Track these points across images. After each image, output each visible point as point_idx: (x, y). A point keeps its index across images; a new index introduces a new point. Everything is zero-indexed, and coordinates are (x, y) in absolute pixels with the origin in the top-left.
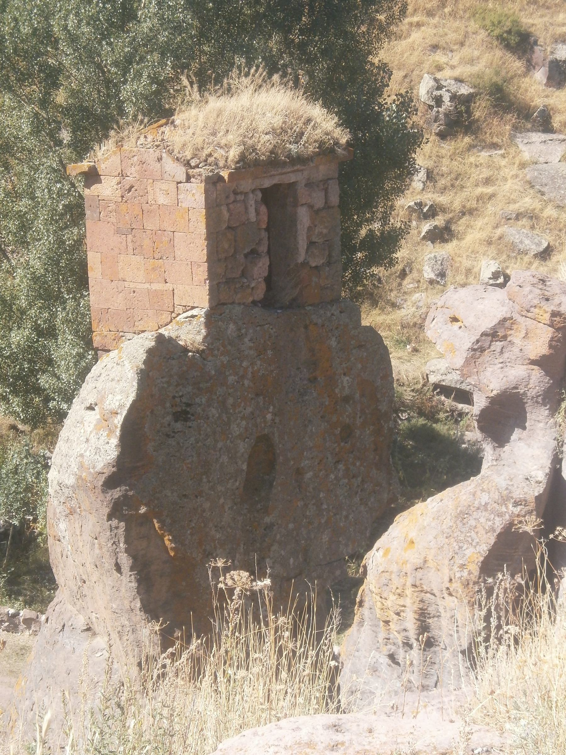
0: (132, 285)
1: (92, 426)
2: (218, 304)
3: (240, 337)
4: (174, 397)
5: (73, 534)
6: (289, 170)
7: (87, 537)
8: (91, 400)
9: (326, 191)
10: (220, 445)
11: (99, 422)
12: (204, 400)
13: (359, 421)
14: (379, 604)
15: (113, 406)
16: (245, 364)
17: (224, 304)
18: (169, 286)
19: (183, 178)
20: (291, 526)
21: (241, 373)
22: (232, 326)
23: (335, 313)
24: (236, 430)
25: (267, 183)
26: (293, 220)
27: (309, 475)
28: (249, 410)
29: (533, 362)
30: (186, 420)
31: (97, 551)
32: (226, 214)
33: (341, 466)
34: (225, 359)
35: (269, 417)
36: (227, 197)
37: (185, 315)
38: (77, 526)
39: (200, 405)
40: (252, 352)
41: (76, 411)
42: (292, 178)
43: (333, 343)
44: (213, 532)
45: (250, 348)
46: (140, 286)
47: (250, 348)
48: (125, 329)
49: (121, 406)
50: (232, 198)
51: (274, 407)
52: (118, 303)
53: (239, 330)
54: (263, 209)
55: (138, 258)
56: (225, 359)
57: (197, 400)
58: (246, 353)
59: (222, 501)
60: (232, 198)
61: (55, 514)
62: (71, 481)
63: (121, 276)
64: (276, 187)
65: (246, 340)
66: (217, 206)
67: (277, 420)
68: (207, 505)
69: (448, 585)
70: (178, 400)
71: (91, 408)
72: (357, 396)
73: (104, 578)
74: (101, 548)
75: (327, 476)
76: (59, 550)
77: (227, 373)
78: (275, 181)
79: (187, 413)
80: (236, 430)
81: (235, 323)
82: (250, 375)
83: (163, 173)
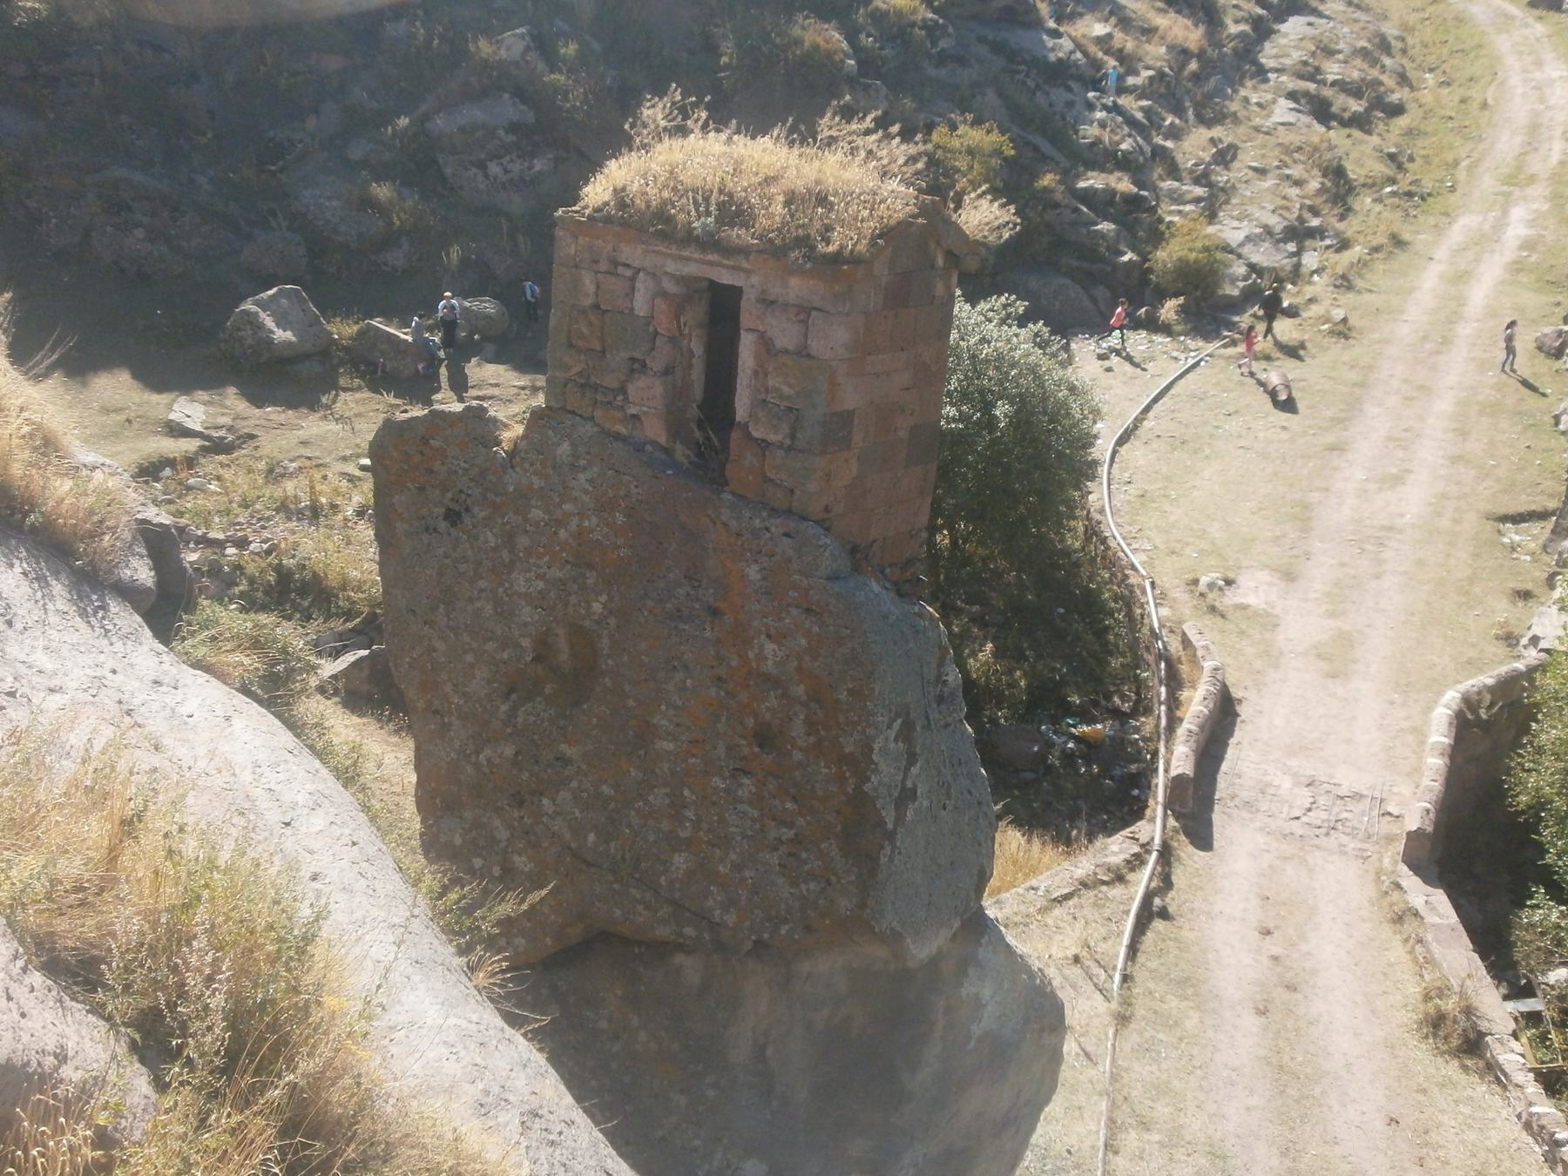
2: (563, 409)
3: (573, 467)
4: (461, 491)
6: (696, 256)
10: (482, 584)
16: (567, 507)
17: (573, 412)
21: (558, 514)
22: (565, 447)
23: (773, 529)
25: (671, 267)
28: (560, 575)
30: (454, 524)
34: (537, 483)
35: (597, 607)
36: (596, 262)
39: (473, 516)
40: (586, 499)
42: (726, 278)
43: (753, 572)
44: (448, 688)
45: (586, 492)
47: (586, 492)
50: (603, 266)
51: (611, 598)
53: (576, 457)
56: (537, 483)
59: (469, 658)
60: (603, 266)
65: (582, 477)
66: (576, 267)
70: (463, 496)
77: (533, 502)
79: (459, 514)
80: (520, 581)
81: (572, 444)
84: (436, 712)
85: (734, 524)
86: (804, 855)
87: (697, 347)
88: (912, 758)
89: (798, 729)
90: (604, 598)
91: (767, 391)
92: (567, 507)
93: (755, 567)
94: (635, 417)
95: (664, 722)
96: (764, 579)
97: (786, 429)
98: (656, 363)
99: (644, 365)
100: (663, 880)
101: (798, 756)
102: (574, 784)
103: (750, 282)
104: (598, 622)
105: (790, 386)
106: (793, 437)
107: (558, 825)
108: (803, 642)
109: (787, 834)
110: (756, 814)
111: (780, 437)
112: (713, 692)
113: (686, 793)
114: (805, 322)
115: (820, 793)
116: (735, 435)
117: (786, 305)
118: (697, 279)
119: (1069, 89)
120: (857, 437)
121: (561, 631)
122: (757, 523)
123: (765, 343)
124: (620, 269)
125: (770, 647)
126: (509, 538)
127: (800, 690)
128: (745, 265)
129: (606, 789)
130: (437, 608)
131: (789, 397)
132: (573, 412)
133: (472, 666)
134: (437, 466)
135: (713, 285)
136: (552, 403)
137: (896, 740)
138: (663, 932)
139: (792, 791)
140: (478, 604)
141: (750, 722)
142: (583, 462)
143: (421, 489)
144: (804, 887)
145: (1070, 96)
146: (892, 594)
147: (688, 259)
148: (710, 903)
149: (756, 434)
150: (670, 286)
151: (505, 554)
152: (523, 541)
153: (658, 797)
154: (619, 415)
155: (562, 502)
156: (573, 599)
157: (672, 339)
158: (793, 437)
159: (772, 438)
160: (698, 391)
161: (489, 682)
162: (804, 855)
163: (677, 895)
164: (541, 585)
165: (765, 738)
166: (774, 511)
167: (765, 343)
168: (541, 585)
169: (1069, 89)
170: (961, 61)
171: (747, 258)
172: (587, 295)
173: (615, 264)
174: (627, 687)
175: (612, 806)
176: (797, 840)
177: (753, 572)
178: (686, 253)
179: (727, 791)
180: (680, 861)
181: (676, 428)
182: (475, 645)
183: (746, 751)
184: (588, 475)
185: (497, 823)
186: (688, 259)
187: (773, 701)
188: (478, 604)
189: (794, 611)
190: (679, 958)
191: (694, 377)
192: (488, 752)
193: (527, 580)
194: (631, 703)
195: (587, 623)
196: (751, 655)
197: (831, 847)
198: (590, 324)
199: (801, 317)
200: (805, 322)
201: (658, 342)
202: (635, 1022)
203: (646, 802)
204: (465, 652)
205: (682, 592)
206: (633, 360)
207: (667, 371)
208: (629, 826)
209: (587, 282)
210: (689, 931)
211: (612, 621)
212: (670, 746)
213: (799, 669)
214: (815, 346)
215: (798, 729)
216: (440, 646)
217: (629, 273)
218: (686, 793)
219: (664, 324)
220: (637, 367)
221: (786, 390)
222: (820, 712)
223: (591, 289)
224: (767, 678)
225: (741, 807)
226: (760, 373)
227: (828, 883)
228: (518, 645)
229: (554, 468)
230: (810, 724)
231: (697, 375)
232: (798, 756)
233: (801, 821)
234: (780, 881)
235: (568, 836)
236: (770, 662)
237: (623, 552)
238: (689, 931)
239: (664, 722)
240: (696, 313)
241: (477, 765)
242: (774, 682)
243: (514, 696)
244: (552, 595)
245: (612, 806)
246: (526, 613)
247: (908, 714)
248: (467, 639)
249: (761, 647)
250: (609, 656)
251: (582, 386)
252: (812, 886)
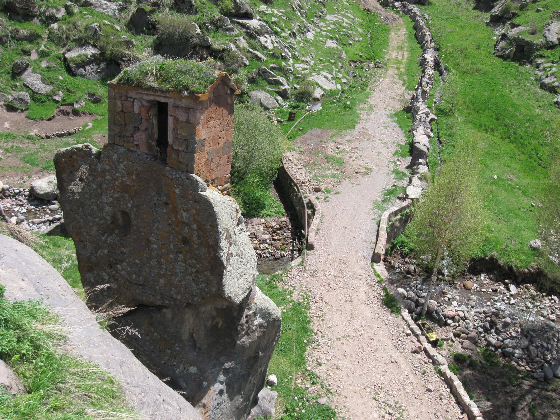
2: (114, 143)
6: (153, 94)
10: (93, 200)
16: (118, 174)
21: (115, 177)
25: (145, 97)
28: (117, 196)
32: (119, 104)
35: (129, 205)
40: (123, 172)
42: (162, 100)
43: (177, 191)
44: (85, 234)
45: (123, 169)
47: (123, 169)
51: (134, 202)
56: (108, 168)
58: (120, 170)
59: (91, 224)
60: (123, 98)
65: (121, 165)
67: (135, 209)
80: (104, 199)
81: (118, 155)
82: (120, 181)
84: (82, 241)
85: (170, 176)
86: (200, 276)
87: (155, 122)
88: (231, 245)
89: (195, 238)
90: (131, 202)
91: (178, 134)
92: (118, 174)
93: (178, 189)
94: (137, 145)
95: (153, 239)
96: (181, 193)
97: (184, 146)
98: (142, 128)
99: (138, 128)
100: (157, 287)
101: (195, 246)
102: (127, 260)
103: (171, 102)
104: (130, 210)
105: (185, 133)
106: (187, 148)
107: (123, 273)
108: (195, 212)
109: (194, 270)
110: (184, 265)
111: (183, 149)
112: (168, 229)
113: (162, 260)
114: (188, 113)
115: (203, 257)
116: (169, 149)
117: (182, 107)
118: (153, 101)
119: (265, 37)
120: (207, 147)
121: (119, 214)
122: (178, 176)
123: (176, 119)
124: (129, 99)
125: (184, 214)
126: (100, 185)
127: (195, 226)
128: (168, 95)
129: (137, 261)
130: (79, 209)
131: (184, 136)
132: (117, 145)
133: (92, 226)
134: (75, 164)
135: (159, 103)
136: (110, 142)
137: (225, 240)
138: (159, 303)
139: (195, 257)
140: (92, 207)
141: (180, 237)
142: (121, 160)
143: (71, 172)
144: (200, 286)
145: (266, 39)
146: (221, 195)
147: (150, 95)
148: (172, 293)
149: (175, 148)
150: (145, 104)
151: (99, 191)
152: (105, 186)
153: (154, 262)
154: (132, 145)
155: (116, 173)
156: (122, 203)
157: (147, 120)
158: (187, 148)
159: (180, 149)
160: (156, 136)
161: (98, 231)
162: (200, 276)
163: (162, 291)
164: (111, 199)
165: (186, 241)
166: (182, 172)
167: (176, 119)
168: (111, 199)
169: (265, 37)
170: (231, 30)
171: (169, 93)
172: (119, 108)
173: (127, 97)
174: (141, 229)
175: (140, 266)
176: (197, 272)
177: (177, 191)
178: (149, 93)
179: (175, 259)
180: (162, 281)
181: (150, 147)
182: (92, 220)
183: (179, 246)
184: (123, 164)
185: (104, 274)
186: (150, 95)
187: (186, 230)
188: (92, 207)
189: (191, 202)
190: (164, 310)
191: (155, 131)
192: (99, 252)
193: (107, 198)
194: (143, 234)
195: (127, 210)
196: (179, 216)
197: (208, 273)
198: (121, 117)
199: (187, 111)
200: (188, 113)
201: (143, 121)
202: (153, 330)
203: (150, 264)
204: (89, 222)
205: (155, 198)
206: (135, 127)
207: (146, 129)
208: (145, 272)
209: (119, 103)
210: (167, 302)
211: (135, 209)
212: (155, 246)
213: (194, 220)
214: (192, 120)
215: (195, 238)
216: (82, 221)
217: (132, 100)
218: (162, 260)
219: (144, 114)
220: (137, 129)
221: (184, 134)
222: (201, 233)
223: (120, 105)
224: (185, 223)
225: (179, 263)
226: (175, 129)
227: (208, 284)
228: (106, 219)
229: (112, 162)
230: (199, 237)
231: (156, 131)
232: (195, 246)
233: (198, 266)
234: (193, 284)
235: (127, 276)
236: (185, 218)
237: (136, 187)
238: (167, 302)
239: (153, 239)
240: (153, 112)
241: (96, 257)
242: (187, 224)
243: (106, 235)
244: (115, 202)
245: (140, 266)
246: (107, 209)
247: (228, 232)
248: (90, 218)
249: (182, 214)
250: (135, 220)
251: (120, 136)
252: (203, 285)
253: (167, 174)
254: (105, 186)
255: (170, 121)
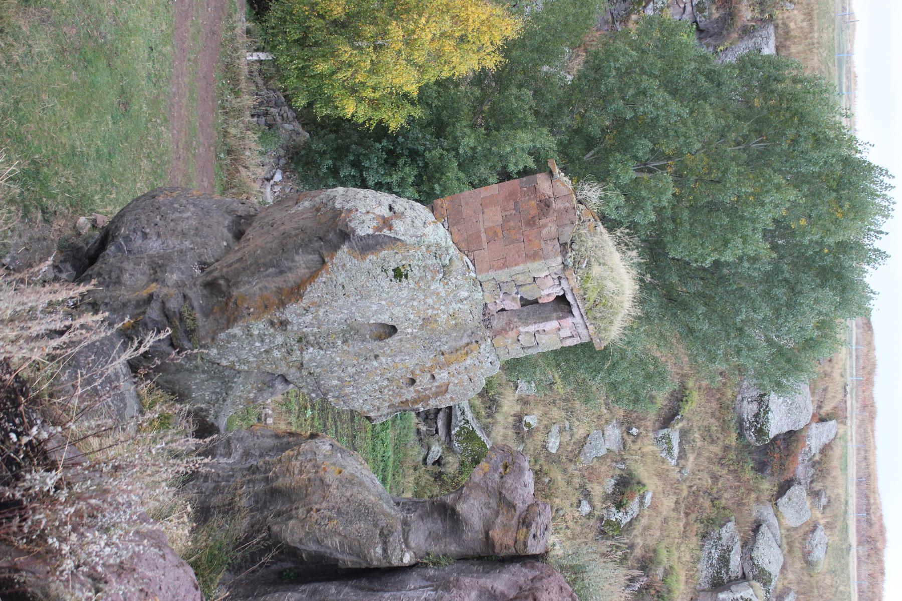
0: (481, 219)
1: (379, 213)
5: (302, 213)
7: (302, 223)
8: (398, 208)
9: (573, 336)
10: (383, 303)
11: (383, 218)
12: (412, 286)
13: (419, 388)
14: (291, 453)
15: (395, 226)
16: (442, 308)
18: (485, 246)
19: (562, 241)
20: (338, 359)
24: (396, 311)
25: (569, 298)
26: (547, 319)
27: (375, 363)
28: (412, 317)
29: (487, 534)
31: (293, 233)
32: (543, 275)
33: (386, 383)
37: (468, 261)
38: (309, 214)
41: (386, 198)
46: (481, 225)
48: (450, 220)
49: (396, 232)
50: (556, 277)
52: (466, 212)
54: (552, 298)
55: (500, 221)
56: (443, 294)
57: (411, 281)
61: (314, 197)
62: (338, 206)
63: (486, 210)
64: (568, 304)
65: (459, 305)
67: (409, 336)
68: (341, 302)
69: (314, 509)
71: (391, 208)
72: (436, 384)
73: (276, 242)
74: (296, 235)
75: (377, 375)
76: (290, 203)
78: (572, 302)
80: (396, 311)
82: (435, 312)
83: (563, 226)
85: (482, 350)
152: (415, 303)
253: (483, 346)
254: (415, 303)
255: (554, 324)
